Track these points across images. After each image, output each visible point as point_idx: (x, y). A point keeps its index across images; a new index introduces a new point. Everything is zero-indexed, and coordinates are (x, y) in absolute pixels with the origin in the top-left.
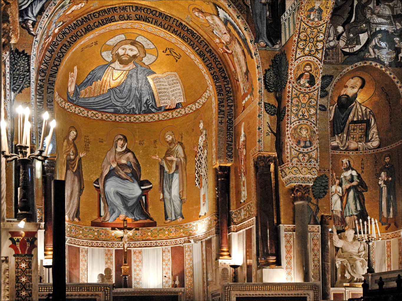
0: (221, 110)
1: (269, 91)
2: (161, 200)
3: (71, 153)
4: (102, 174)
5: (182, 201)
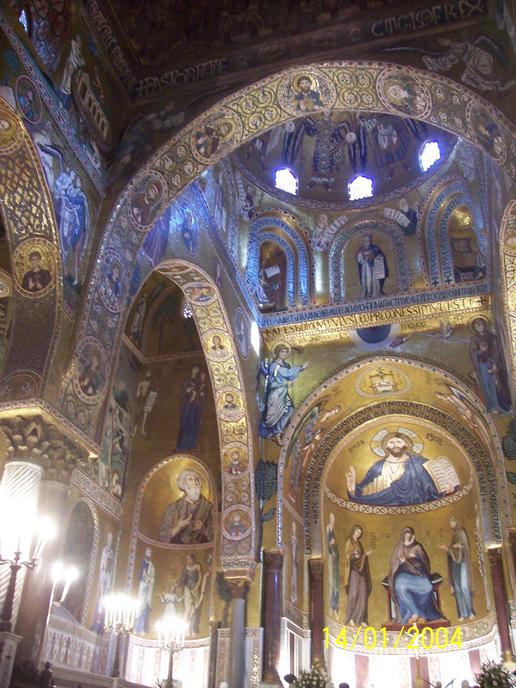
1: (511, 459)
2: (452, 595)
3: (356, 552)
4: (391, 571)
5: (472, 594)
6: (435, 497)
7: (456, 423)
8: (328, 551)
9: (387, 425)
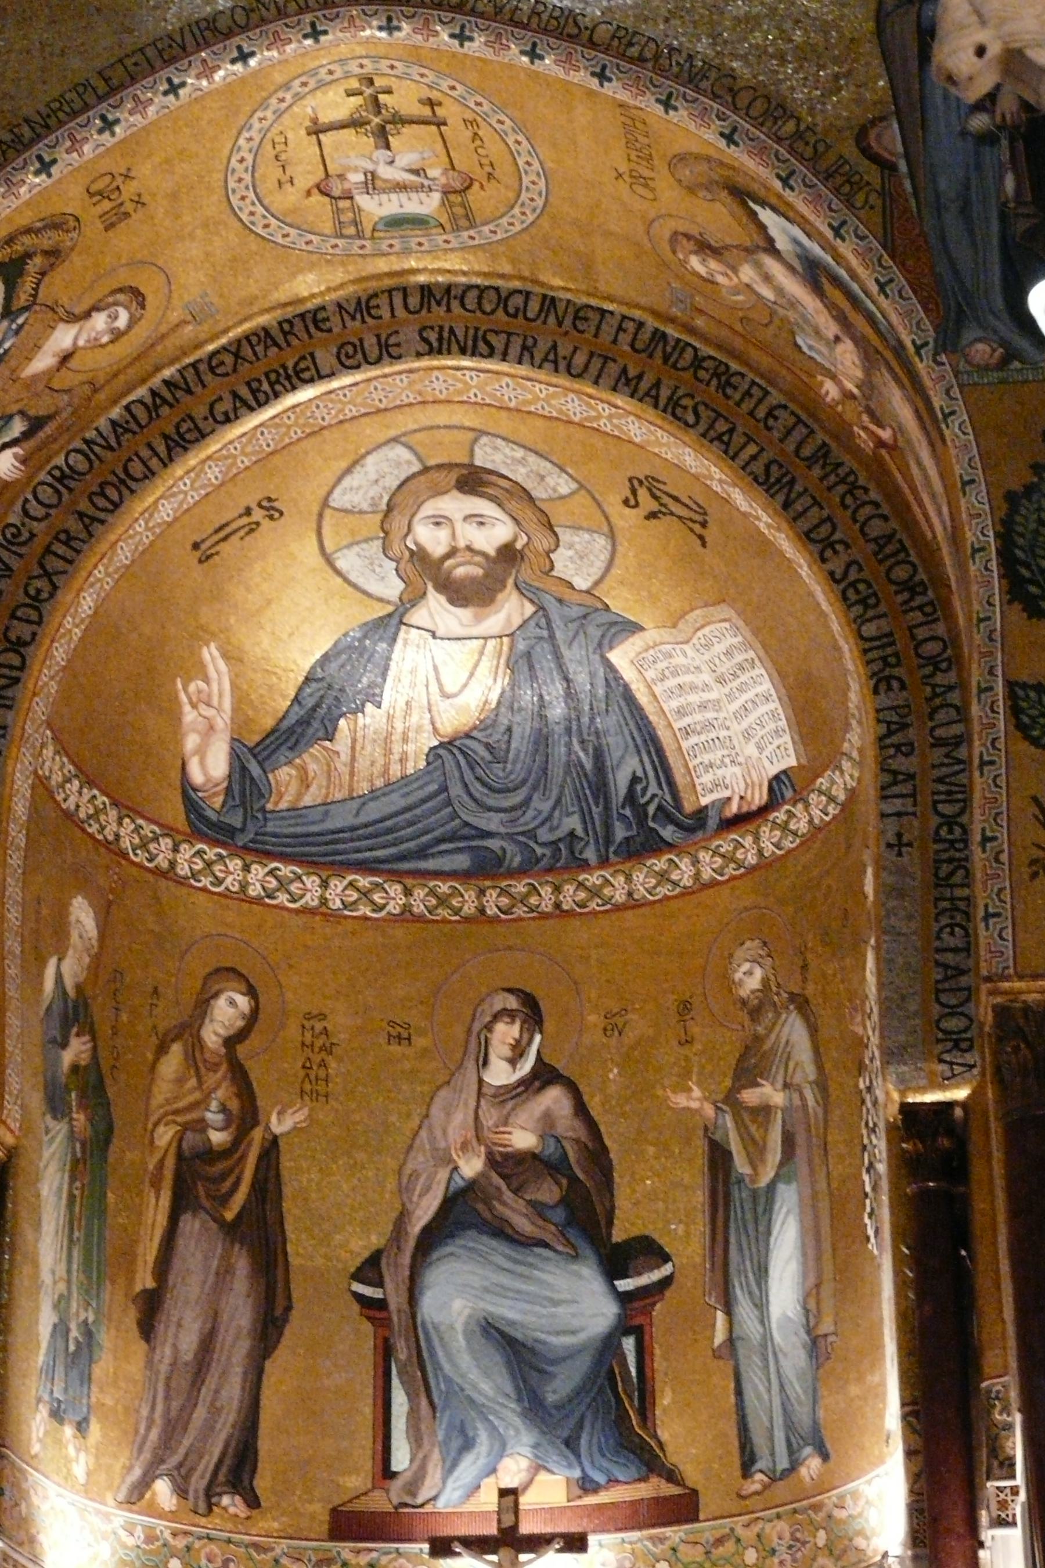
0: (895, 773)
2: (717, 1354)
3: (213, 1117)
6: (668, 832)
7: (785, 419)
8: (36, 1100)
9: (406, 422)
